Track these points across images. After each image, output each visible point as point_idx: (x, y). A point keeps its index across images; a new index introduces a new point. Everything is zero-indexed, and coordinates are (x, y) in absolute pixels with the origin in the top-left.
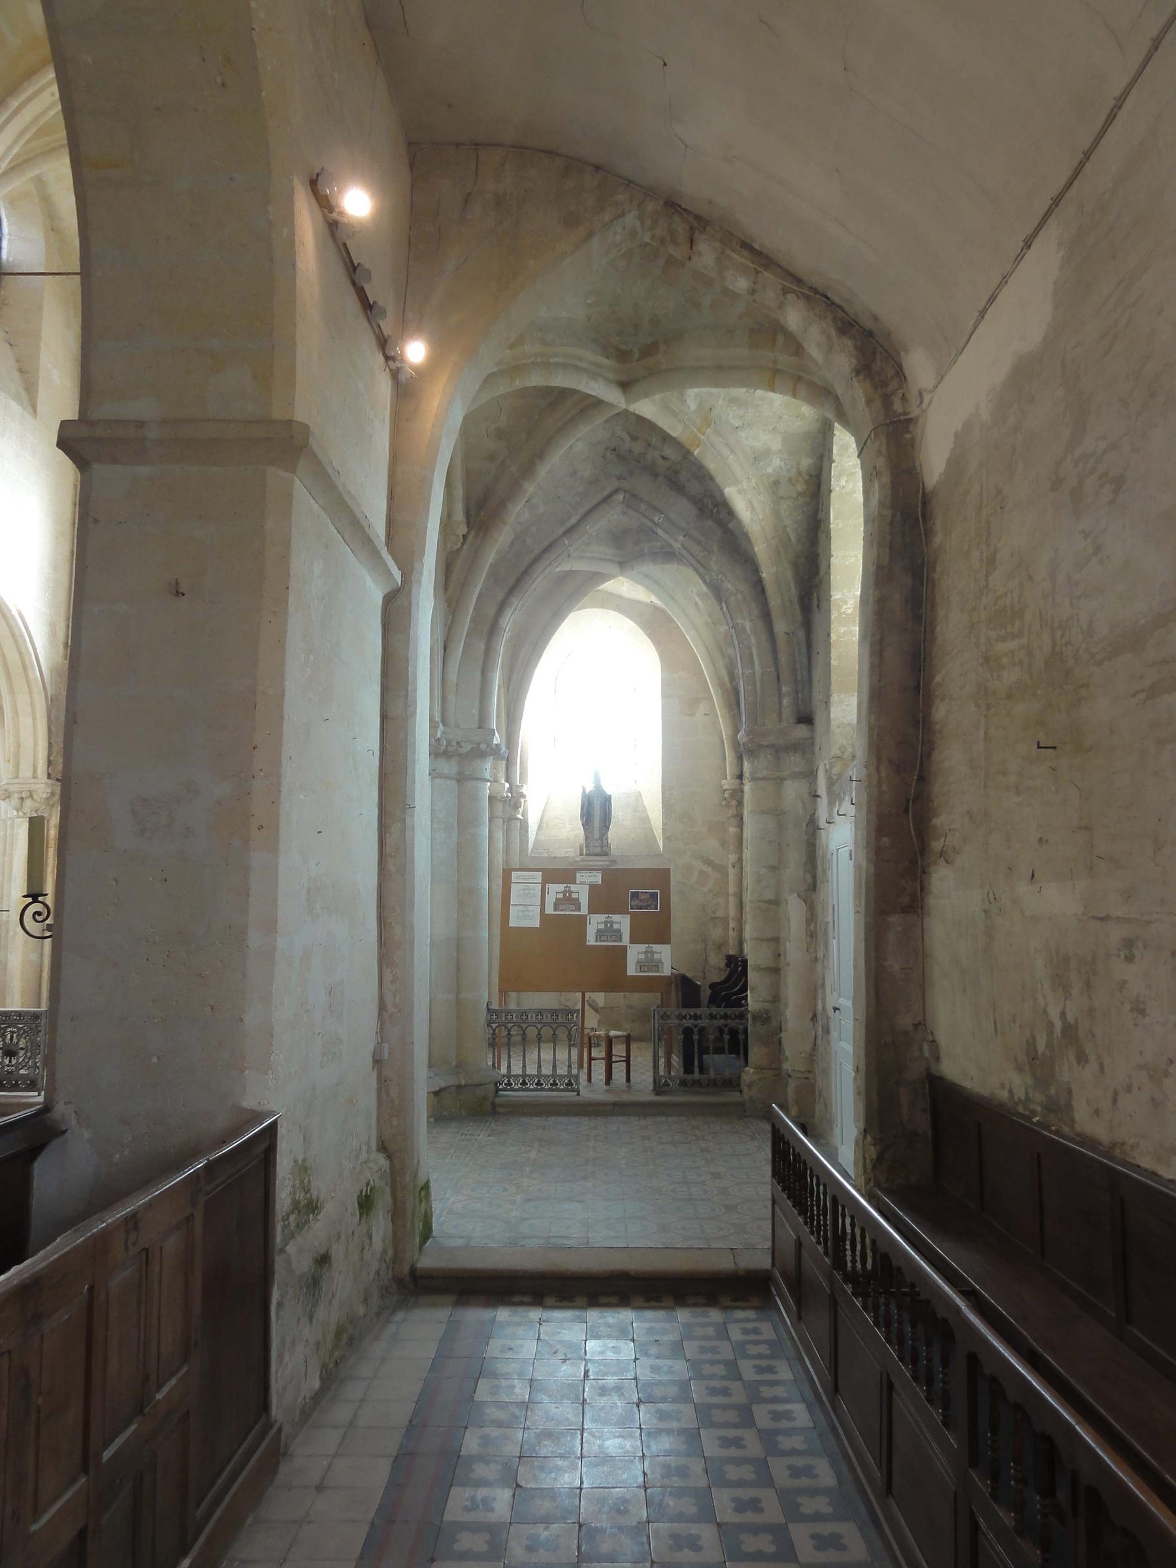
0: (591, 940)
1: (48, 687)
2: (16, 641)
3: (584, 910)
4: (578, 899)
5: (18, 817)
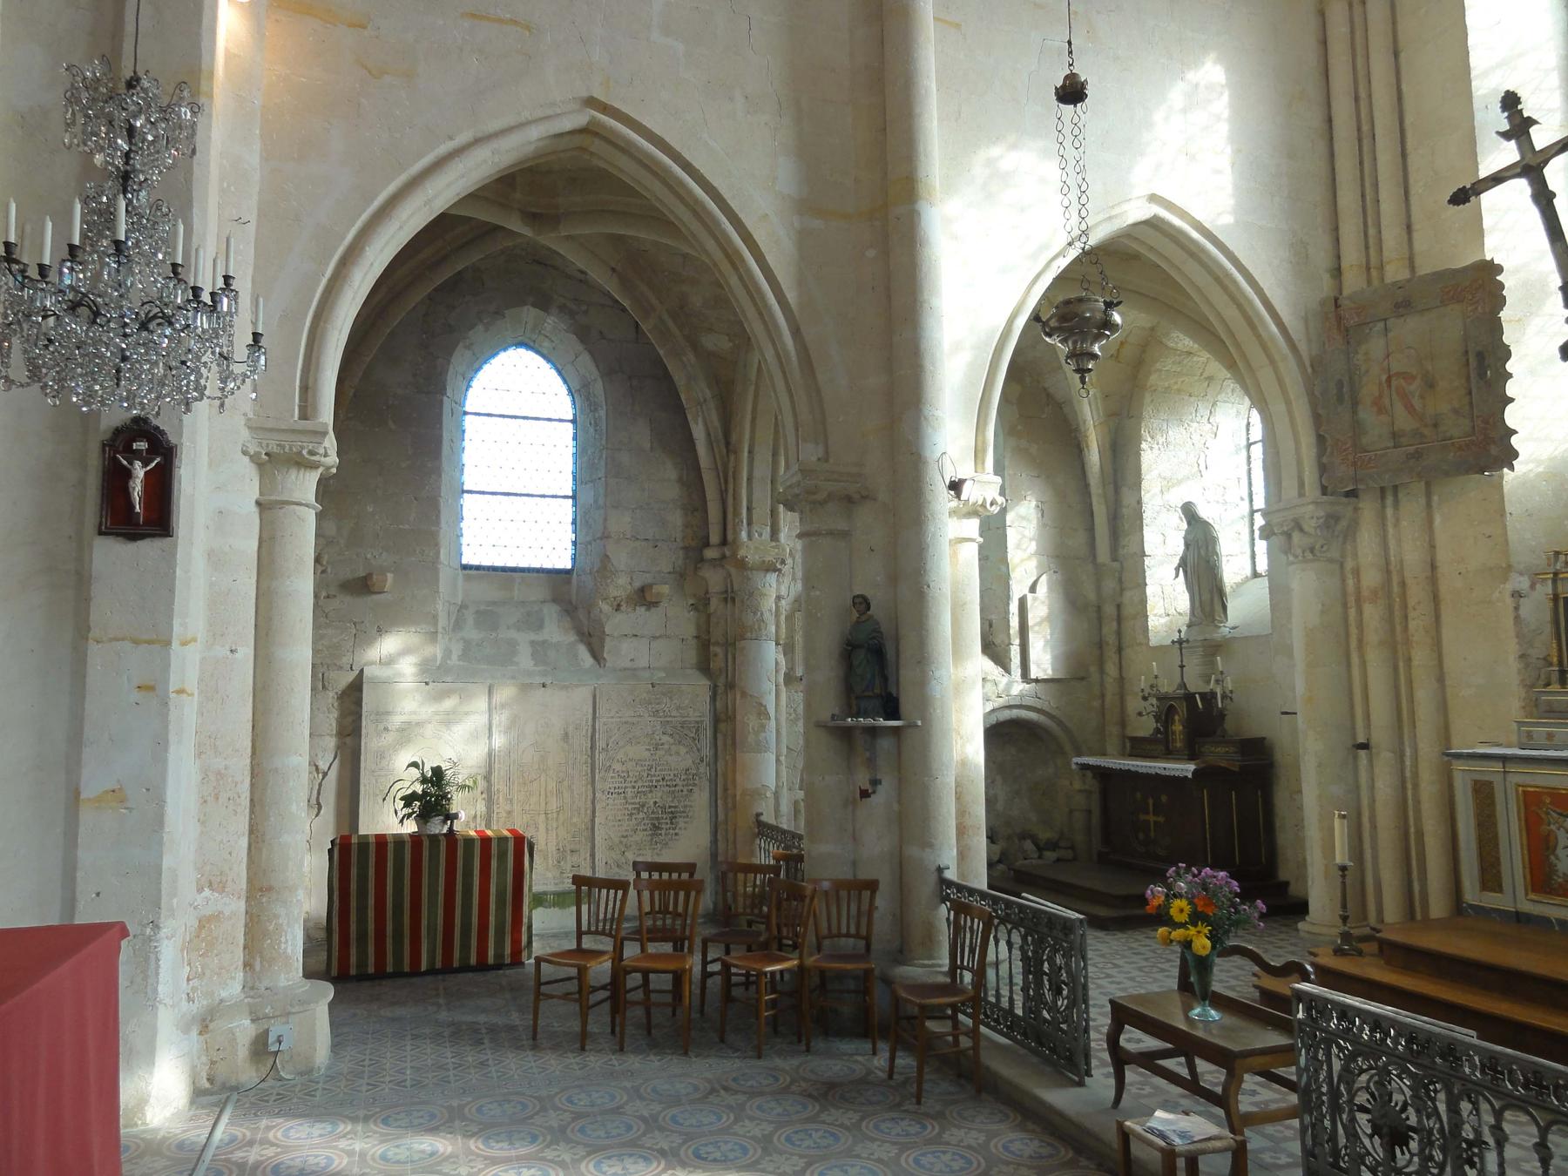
1: (1303, 347)
2: (1225, 288)
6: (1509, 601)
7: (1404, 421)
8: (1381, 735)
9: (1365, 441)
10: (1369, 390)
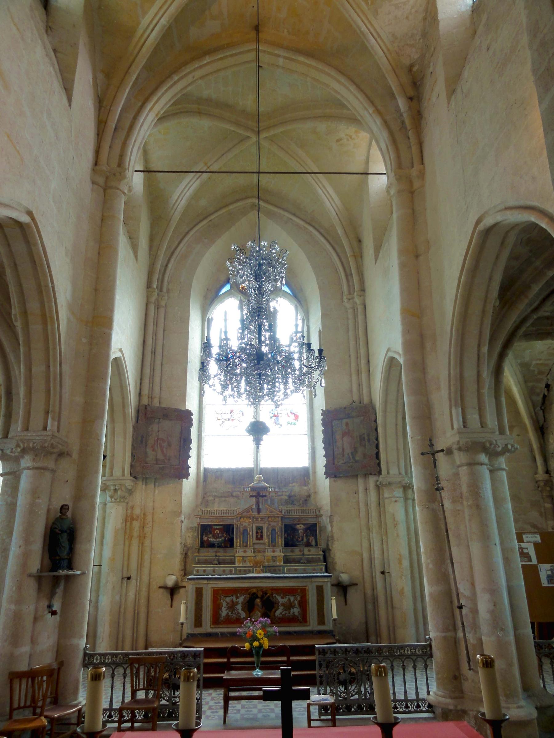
0: (545, 583)
3: (534, 561)
4: (528, 554)
5: (111, 502)
6: (180, 523)
7: (160, 456)
8: (133, 574)
9: (148, 459)
10: (151, 442)
